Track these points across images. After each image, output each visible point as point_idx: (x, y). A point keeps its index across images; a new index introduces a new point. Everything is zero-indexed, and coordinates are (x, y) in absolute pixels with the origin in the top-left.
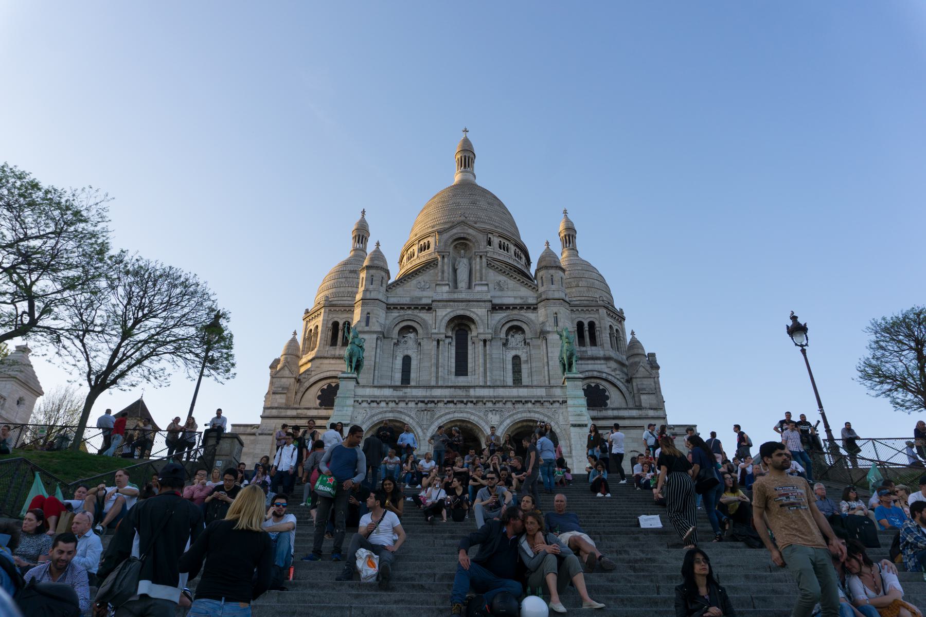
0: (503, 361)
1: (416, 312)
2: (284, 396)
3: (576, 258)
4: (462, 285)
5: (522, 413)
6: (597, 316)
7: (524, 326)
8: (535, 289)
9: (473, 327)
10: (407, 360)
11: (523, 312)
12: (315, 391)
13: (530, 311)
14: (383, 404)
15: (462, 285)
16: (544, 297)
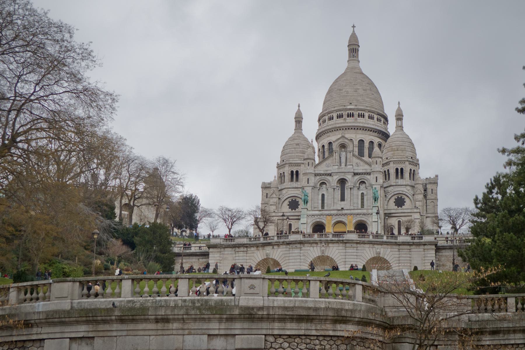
0: (358, 195)
1: (326, 176)
2: (275, 206)
3: (400, 133)
4: (343, 165)
5: (359, 218)
6: (404, 165)
7: (366, 181)
8: (370, 165)
9: (347, 182)
10: (323, 195)
11: (365, 176)
12: (287, 202)
13: (368, 175)
14: (316, 216)
15: (343, 165)
16: (373, 170)
